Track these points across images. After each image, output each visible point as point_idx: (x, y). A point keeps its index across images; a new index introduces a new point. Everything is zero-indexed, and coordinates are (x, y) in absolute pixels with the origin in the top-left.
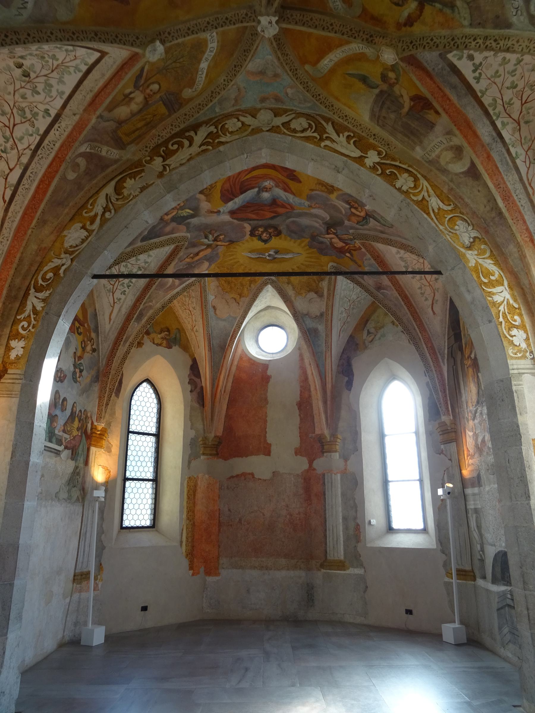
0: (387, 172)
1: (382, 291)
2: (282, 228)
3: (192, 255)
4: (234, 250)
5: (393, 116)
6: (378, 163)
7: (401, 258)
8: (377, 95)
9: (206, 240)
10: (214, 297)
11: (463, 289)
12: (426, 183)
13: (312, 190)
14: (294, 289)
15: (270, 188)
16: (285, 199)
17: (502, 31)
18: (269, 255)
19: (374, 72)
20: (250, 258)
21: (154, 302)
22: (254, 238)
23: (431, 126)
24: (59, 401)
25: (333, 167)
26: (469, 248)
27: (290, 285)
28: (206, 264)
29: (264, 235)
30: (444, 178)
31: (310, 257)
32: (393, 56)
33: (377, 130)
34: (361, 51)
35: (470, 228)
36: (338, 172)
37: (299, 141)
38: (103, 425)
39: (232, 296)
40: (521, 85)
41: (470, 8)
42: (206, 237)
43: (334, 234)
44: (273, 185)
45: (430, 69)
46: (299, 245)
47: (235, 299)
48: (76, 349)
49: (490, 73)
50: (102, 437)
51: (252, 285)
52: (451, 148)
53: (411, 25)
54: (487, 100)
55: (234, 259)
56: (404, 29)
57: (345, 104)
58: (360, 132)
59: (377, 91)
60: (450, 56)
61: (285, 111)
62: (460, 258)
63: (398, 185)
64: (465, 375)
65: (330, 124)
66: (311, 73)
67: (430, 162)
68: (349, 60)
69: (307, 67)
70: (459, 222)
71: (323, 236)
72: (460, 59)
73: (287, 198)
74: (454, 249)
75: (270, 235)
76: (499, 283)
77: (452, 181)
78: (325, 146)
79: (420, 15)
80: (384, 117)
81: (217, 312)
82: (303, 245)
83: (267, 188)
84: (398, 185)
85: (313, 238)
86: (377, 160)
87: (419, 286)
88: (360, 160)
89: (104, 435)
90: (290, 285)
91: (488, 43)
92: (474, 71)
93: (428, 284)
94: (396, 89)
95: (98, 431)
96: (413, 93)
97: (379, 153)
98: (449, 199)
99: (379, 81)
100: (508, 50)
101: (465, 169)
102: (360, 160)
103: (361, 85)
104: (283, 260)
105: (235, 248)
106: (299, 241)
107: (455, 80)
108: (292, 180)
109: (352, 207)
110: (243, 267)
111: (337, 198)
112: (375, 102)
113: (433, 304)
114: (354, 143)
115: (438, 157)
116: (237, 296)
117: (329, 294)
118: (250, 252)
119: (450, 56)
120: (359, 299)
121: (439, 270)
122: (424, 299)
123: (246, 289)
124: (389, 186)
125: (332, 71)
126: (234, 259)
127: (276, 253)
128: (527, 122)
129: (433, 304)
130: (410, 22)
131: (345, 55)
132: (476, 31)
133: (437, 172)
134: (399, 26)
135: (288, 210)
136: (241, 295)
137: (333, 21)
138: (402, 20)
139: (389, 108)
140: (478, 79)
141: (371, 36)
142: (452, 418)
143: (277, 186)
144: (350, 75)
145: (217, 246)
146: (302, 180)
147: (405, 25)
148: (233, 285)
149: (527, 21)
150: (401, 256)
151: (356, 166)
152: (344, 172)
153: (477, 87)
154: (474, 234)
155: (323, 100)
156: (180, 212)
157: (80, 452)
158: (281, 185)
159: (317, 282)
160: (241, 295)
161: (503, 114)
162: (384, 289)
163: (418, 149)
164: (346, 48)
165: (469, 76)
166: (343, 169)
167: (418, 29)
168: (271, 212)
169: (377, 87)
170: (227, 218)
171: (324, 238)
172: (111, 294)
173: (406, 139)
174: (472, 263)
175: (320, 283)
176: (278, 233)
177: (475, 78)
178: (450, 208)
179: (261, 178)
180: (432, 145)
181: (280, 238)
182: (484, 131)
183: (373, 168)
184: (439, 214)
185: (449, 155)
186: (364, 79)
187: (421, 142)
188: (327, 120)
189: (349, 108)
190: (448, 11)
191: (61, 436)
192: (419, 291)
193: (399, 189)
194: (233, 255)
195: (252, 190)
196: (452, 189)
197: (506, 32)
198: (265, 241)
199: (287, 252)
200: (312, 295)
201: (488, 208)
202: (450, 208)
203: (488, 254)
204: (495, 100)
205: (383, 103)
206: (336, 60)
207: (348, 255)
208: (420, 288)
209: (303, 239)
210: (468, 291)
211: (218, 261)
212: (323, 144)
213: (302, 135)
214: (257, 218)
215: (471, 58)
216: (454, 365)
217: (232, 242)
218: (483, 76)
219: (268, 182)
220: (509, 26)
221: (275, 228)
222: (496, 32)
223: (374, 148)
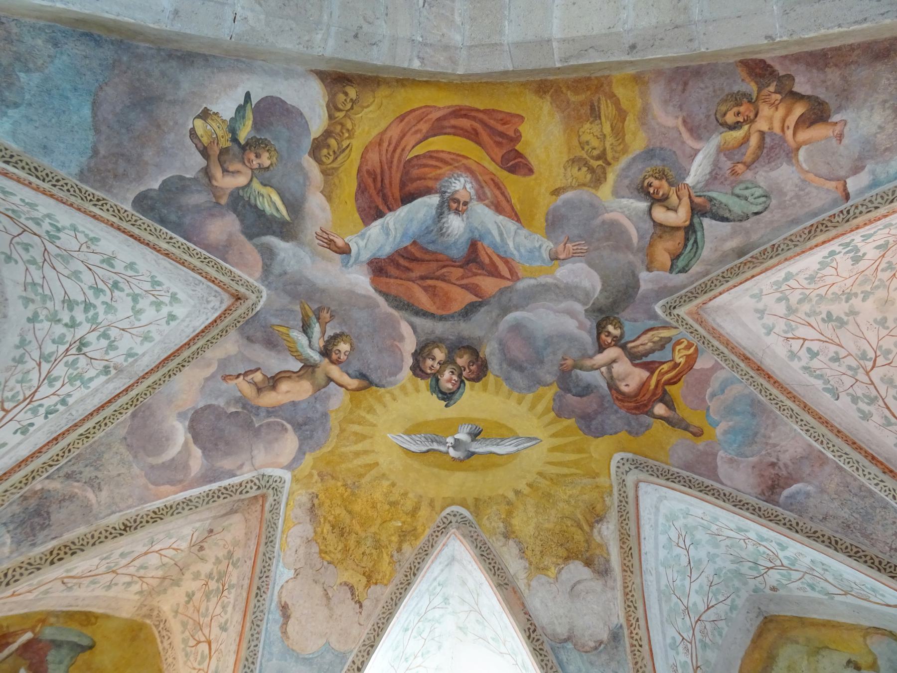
1: (786, 492)
2: (489, 350)
3: (258, 377)
4: (369, 417)
7: (806, 368)
9: (303, 339)
10: (291, 574)
13: (556, 192)
14: (522, 551)
15: (466, 204)
16: (498, 239)
18: (457, 444)
20: (407, 451)
21: (104, 494)
22: (423, 384)
27: (511, 542)
28: (290, 443)
29: (447, 374)
31: (558, 456)
39: (346, 576)
42: (306, 329)
44: (472, 192)
46: (532, 407)
47: (352, 589)
51: (406, 547)
55: (366, 452)
73: (501, 234)
75: (460, 375)
81: (290, 629)
82: (540, 408)
83: (458, 201)
85: (566, 379)
90: (511, 542)
104: (492, 461)
105: (371, 410)
106: (530, 396)
108: (512, 170)
110: (386, 483)
111: (616, 193)
116: (358, 581)
117: (627, 569)
118: (408, 432)
120: (711, 615)
123: (386, 559)
126: (366, 452)
127: (475, 435)
136: (370, 578)
143: (481, 198)
145: (330, 380)
146: (533, 162)
148: (352, 543)
150: (803, 363)
156: (256, 185)
158: (489, 194)
159: (586, 528)
160: (370, 578)
162: (791, 480)
168: (465, 287)
170: (360, 280)
175: (595, 531)
176: (480, 371)
179: (446, 163)
181: (485, 389)
194: (364, 437)
195: (426, 199)
198: (448, 397)
199: (503, 433)
200: (577, 570)
207: (660, 409)
209: (541, 389)
211: (325, 450)
214: (432, 309)
217: (367, 381)
221: (473, 351)
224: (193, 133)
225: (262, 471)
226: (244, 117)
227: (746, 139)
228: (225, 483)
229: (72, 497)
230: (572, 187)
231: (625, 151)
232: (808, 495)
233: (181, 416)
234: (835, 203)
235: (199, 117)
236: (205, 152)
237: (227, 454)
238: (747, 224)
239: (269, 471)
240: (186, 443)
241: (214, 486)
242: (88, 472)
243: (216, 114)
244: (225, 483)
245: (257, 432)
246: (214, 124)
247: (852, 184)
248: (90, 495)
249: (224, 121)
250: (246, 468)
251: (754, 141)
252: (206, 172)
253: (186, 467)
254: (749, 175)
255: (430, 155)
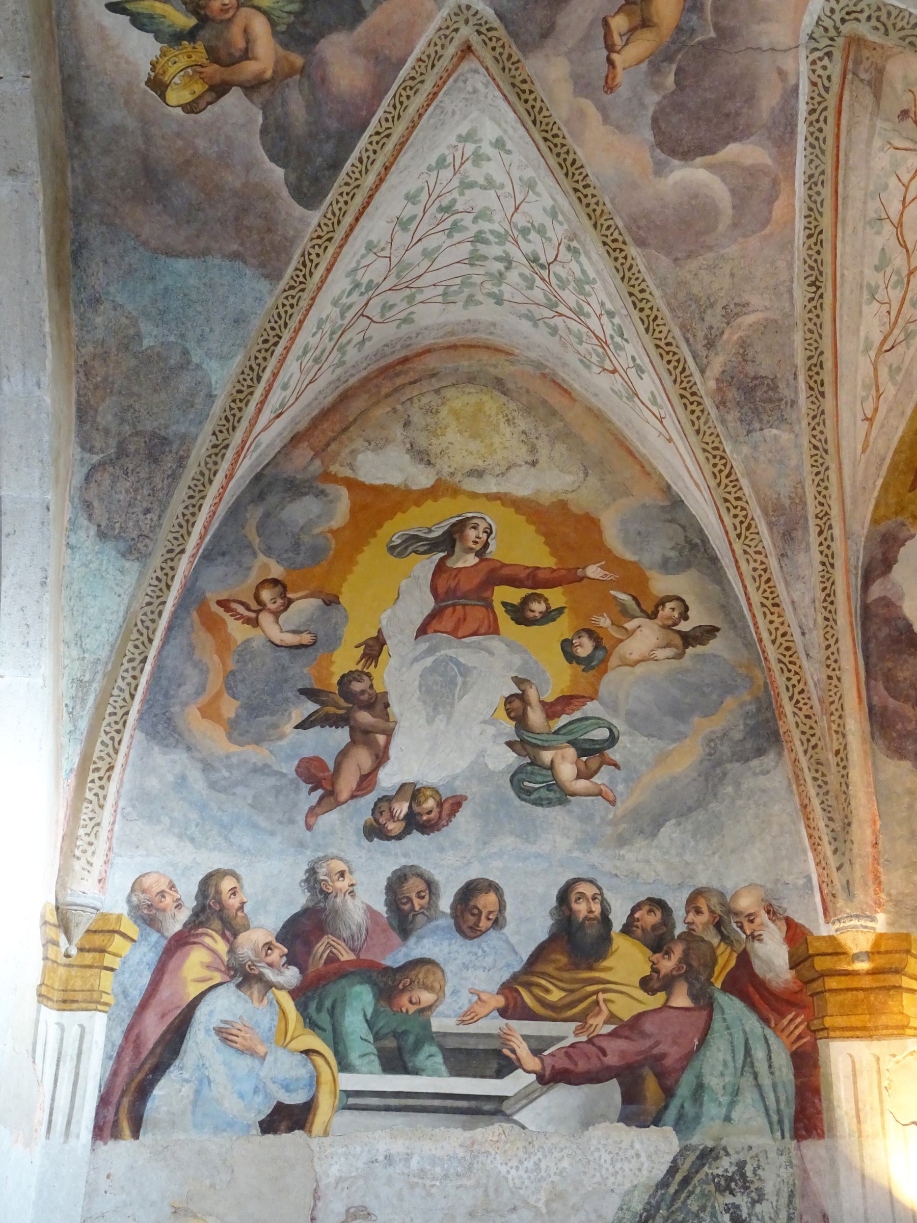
3: (619, 23)
21: (756, 300)
24: (432, 905)
38: (881, 923)
48: (518, 681)
50: (892, 979)
89: (898, 971)
95: (856, 957)
157: (713, 1081)
172: (636, 399)
191: (503, 1038)
224: (191, 108)
225: (803, 38)
226: (151, 17)
228: (803, 109)
229: (744, 344)
233: (660, 169)
235: (163, 96)
236: (219, 90)
237: (751, 99)
239: (808, 21)
240: (710, 167)
241: (802, 128)
242: (714, 318)
243: (153, 66)
244: (803, 109)
245: (725, 34)
246: (172, 70)
248: (751, 319)
249: (163, 54)
250: (787, 63)
252: (251, 88)
253: (753, 172)
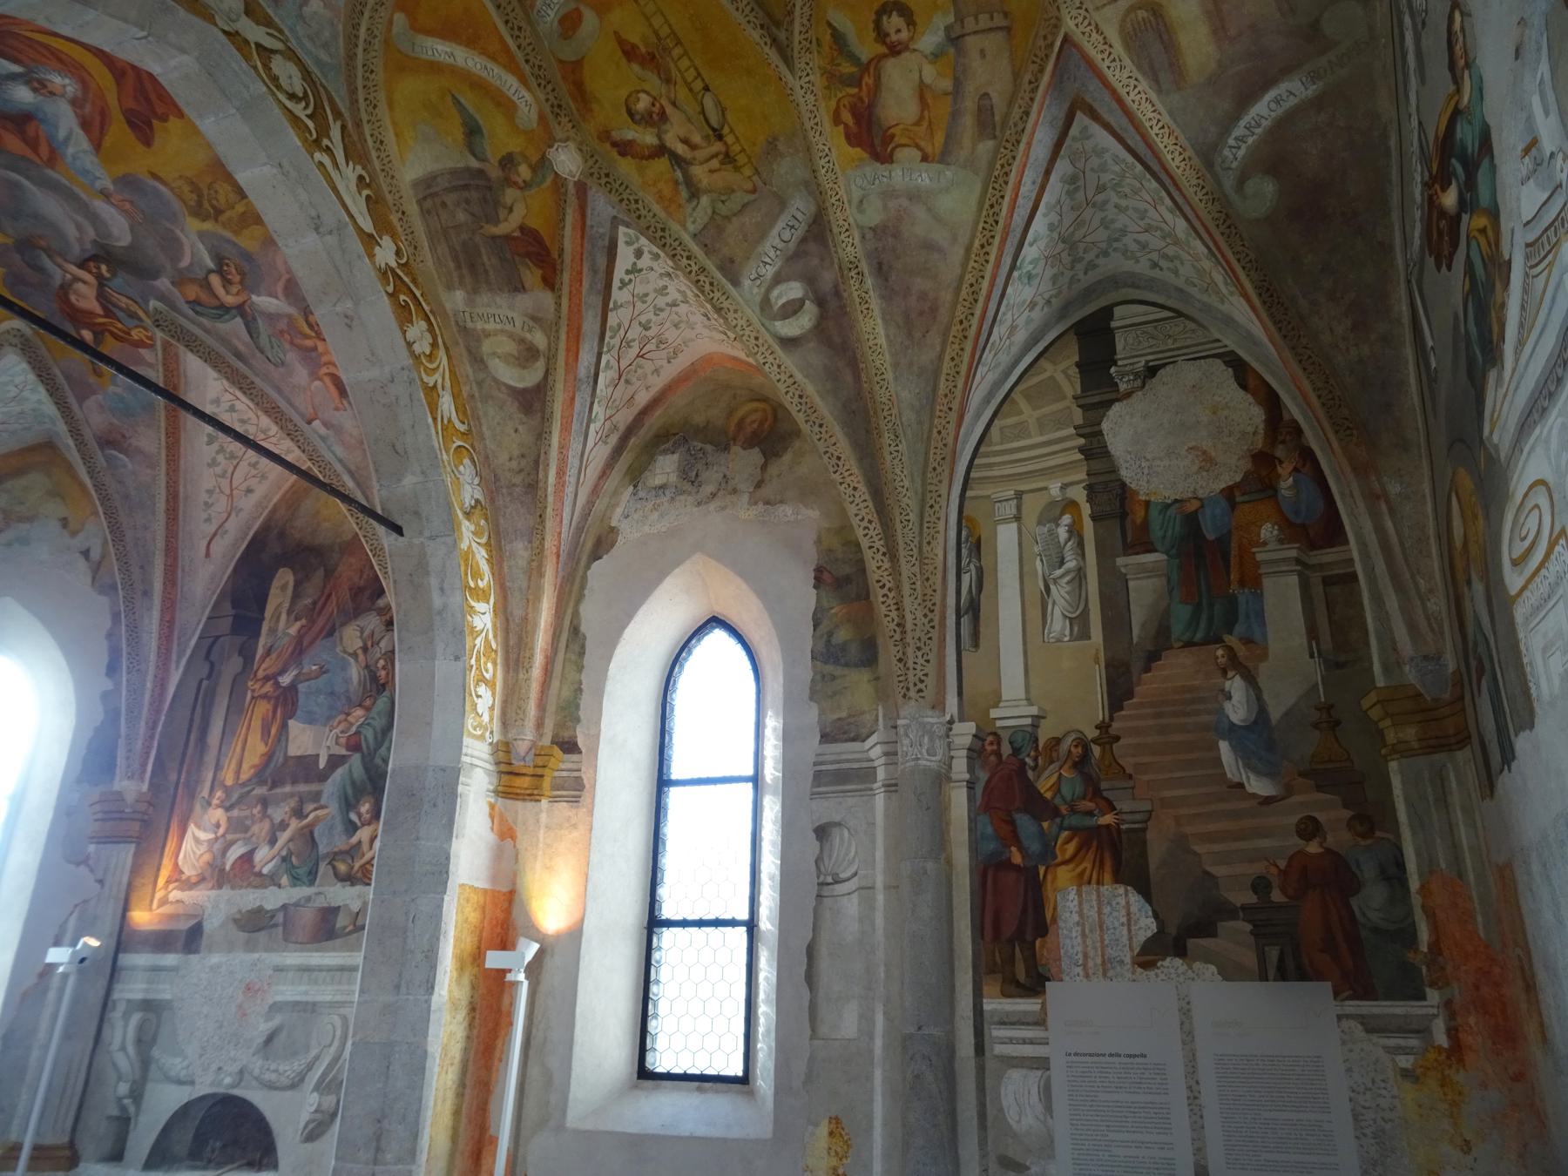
0: (402, 297)
1: (115, 453)
5: (461, 216)
6: (392, 270)
8: (468, 169)
11: (434, 582)
12: (445, 361)
15: (52, 93)
17: (724, 280)
19: (500, 139)
23: (518, 287)
25: (314, 214)
26: (468, 515)
30: (470, 371)
32: (574, 169)
33: (413, 209)
34: (515, 98)
35: (477, 481)
36: (317, 229)
37: (277, 110)
40: (650, 333)
41: (712, 218)
43: (99, 277)
45: (589, 223)
49: (640, 290)
52: (522, 341)
53: (623, 154)
54: (612, 320)
56: (608, 146)
57: (394, 124)
58: (385, 189)
59: (475, 164)
60: (622, 229)
61: (268, 22)
62: (452, 528)
63: (410, 335)
64: (236, 708)
65: (339, 124)
66: (395, 30)
67: (464, 330)
68: (478, 85)
69: (400, 19)
70: (467, 461)
71: (59, 260)
72: (628, 243)
74: (449, 506)
76: (482, 595)
77: (480, 384)
78: (321, 163)
79: (642, 158)
80: (444, 205)
83: (45, 87)
84: (410, 335)
86: (393, 264)
87: (210, 486)
88: (369, 241)
91: (702, 278)
92: (628, 272)
93: (228, 492)
94: (510, 195)
96: (534, 223)
97: (398, 253)
98: (465, 413)
99: (494, 157)
100: (718, 310)
101: (520, 385)
102: (369, 241)
103: (459, 134)
107: (602, 262)
109: (220, 272)
112: (453, 172)
113: (215, 534)
114: (368, 197)
115: (487, 335)
119: (622, 229)
121: (399, 523)
122: (205, 516)
124: (394, 325)
125: (435, 68)
128: (627, 382)
129: (215, 534)
130: (625, 148)
131: (484, 74)
132: (696, 249)
133: (465, 353)
134: (605, 136)
135: (36, 159)
137: (523, 24)
138: (616, 135)
139: (467, 202)
140: (624, 284)
141: (559, 106)
142: (145, 787)
144: (457, 102)
146: (157, 142)
147: (615, 144)
149: (758, 299)
151: (359, 247)
152: (328, 237)
153: (618, 295)
154: (478, 495)
155: (370, 84)
161: (614, 352)
162: (125, 451)
163: (459, 295)
164: (497, 70)
165: (619, 273)
166: (330, 233)
167: (626, 167)
169: (483, 160)
171: (60, 266)
173: (452, 265)
174: (464, 546)
177: (622, 281)
178: (462, 428)
180: (492, 311)
182: (586, 358)
183: (384, 273)
184: (447, 428)
185: (510, 347)
186: (473, 132)
187: (475, 291)
188: (338, 115)
189: (397, 135)
190: (684, 194)
192: (204, 497)
193: (409, 345)
196: (473, 396)
197: (729, 286)
201: (514, 464)
202: (462, 428)
203: (484, 540)
204: (619, 326)
205: (466, 187)
206: (460, 62)
208: (210, 492)
210: (442, 589)
212: (318, 156)
213: (288, 104)
215: (639, 254)
216: (209, 676)
218: (631, 287)
219: (67, 81)
220: (736, 283)
222: (718, 275)
223: (394, 236)
227: (307, 337)
230: (172, 189)
231: (236, 233)
232: (125, 466)
234: (302, 415)
238: (259, 355)
247: (316, 423)
251: (309, 343)
254: (287, 346)
255: (46, 47)
